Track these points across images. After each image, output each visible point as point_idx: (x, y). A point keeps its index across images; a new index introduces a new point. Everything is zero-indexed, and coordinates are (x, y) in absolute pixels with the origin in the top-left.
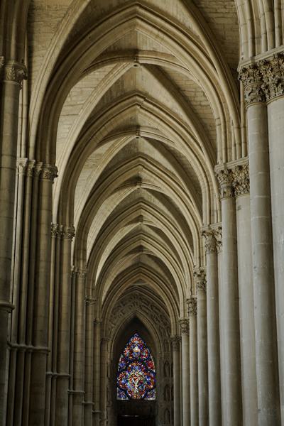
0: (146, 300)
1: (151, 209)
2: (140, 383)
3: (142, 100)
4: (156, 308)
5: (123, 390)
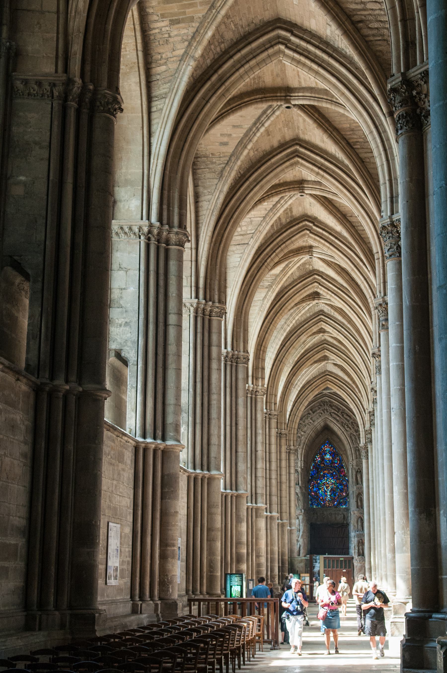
0: (335, 406)
1: (331, 321)
2: (332, 491)
3: (311, 225)
4: (347, 415)
5: (315, 498)
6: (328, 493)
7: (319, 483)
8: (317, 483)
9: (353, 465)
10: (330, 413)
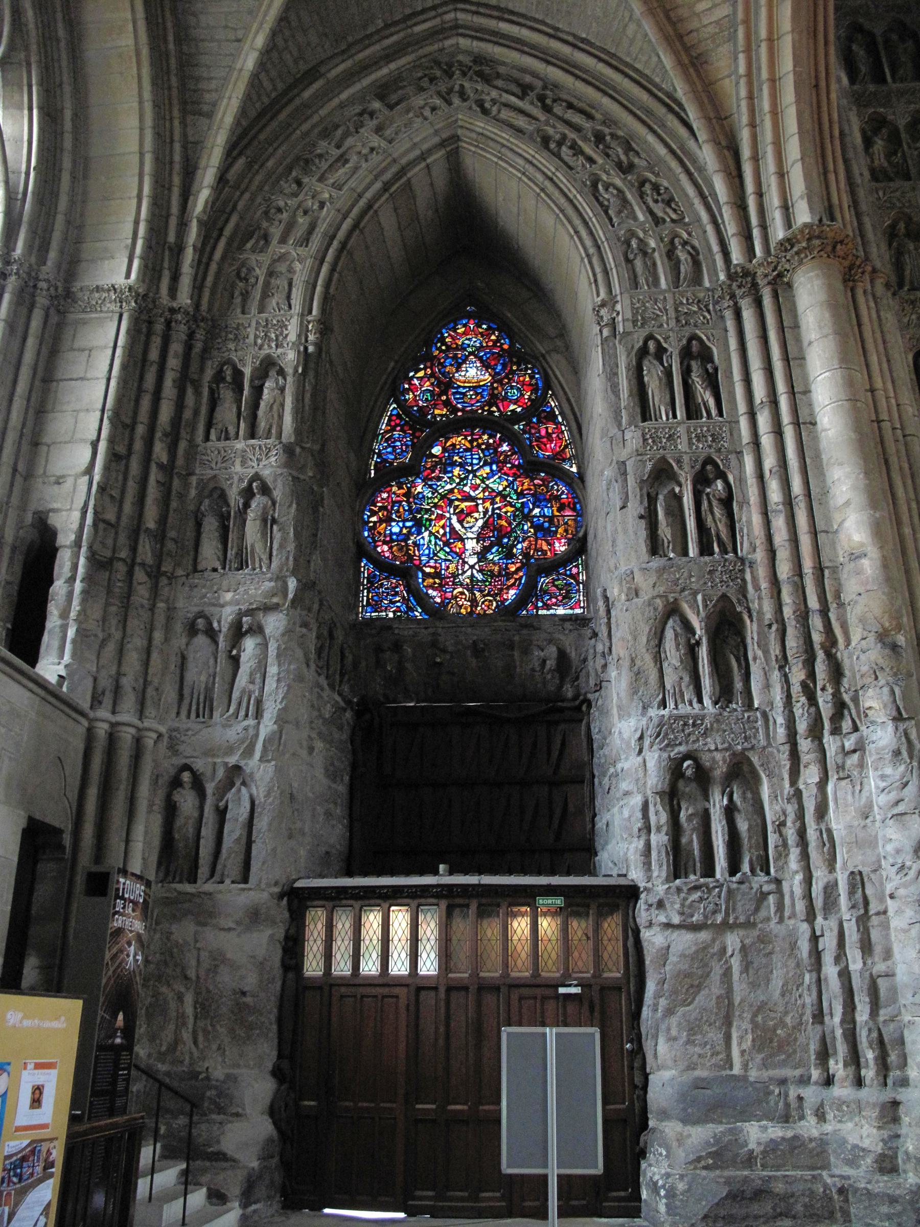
0: (509, 79)
4: (570, 106)
6: (471, 545)
7: (421, 497)
8: (408, 495)
9: (613, 324)
10: (481, 104)
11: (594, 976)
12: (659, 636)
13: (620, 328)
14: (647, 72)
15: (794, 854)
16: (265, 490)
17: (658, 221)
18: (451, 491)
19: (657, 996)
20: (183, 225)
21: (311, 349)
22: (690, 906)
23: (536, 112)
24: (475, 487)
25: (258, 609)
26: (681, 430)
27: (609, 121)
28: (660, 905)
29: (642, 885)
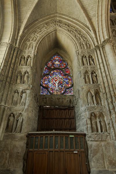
0: (64, 23)
2: (60, 83)
8: (48, 78)
10: (60, 26)
11: (80, 150)
12: (87, 95)
13: (80, 54)
14: (83, 22)
15: (112, 129)
16: (28, 73)
17: (84, 41)
18: (54, 78)
19: (91, 153)
20: (17, 37)
21: (35, 55)
22: (95, 137)
23: (67, 27)
24: (57, 77)
25: (25, 89)
26: (89, 67)
27: (77, 28)
28: (90, 137)
29: (87, 134)
